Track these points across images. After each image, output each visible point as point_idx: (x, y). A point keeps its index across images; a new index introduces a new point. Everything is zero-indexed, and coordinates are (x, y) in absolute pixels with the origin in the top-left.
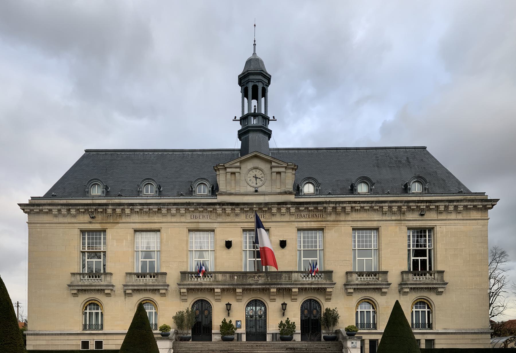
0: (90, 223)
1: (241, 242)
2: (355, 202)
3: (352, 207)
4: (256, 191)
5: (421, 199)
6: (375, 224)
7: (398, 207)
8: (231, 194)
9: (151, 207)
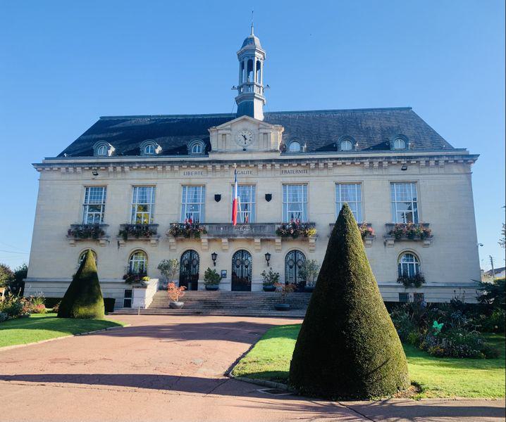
0: (93, 179)
1: (230, 196)
2: (337, 159)
3: (334, 164)
4: (244, 150)
5: (403, 154)
6: (357, 179)
7: (379, 162)
8: (222, 152)
9: (148, 165)
